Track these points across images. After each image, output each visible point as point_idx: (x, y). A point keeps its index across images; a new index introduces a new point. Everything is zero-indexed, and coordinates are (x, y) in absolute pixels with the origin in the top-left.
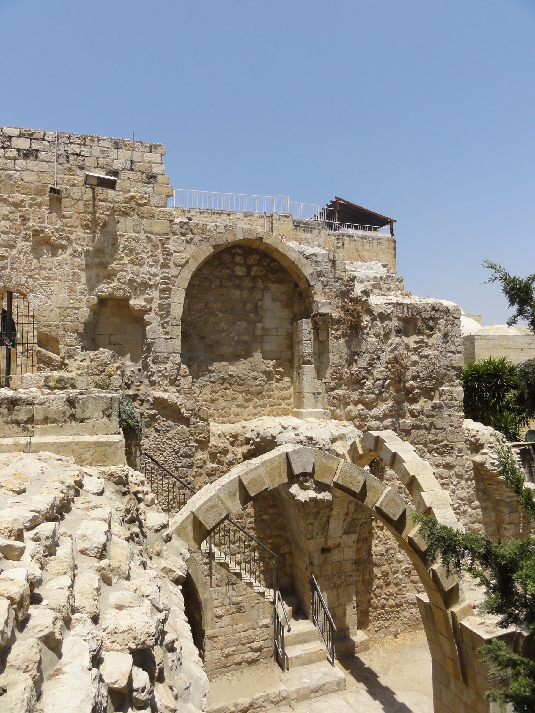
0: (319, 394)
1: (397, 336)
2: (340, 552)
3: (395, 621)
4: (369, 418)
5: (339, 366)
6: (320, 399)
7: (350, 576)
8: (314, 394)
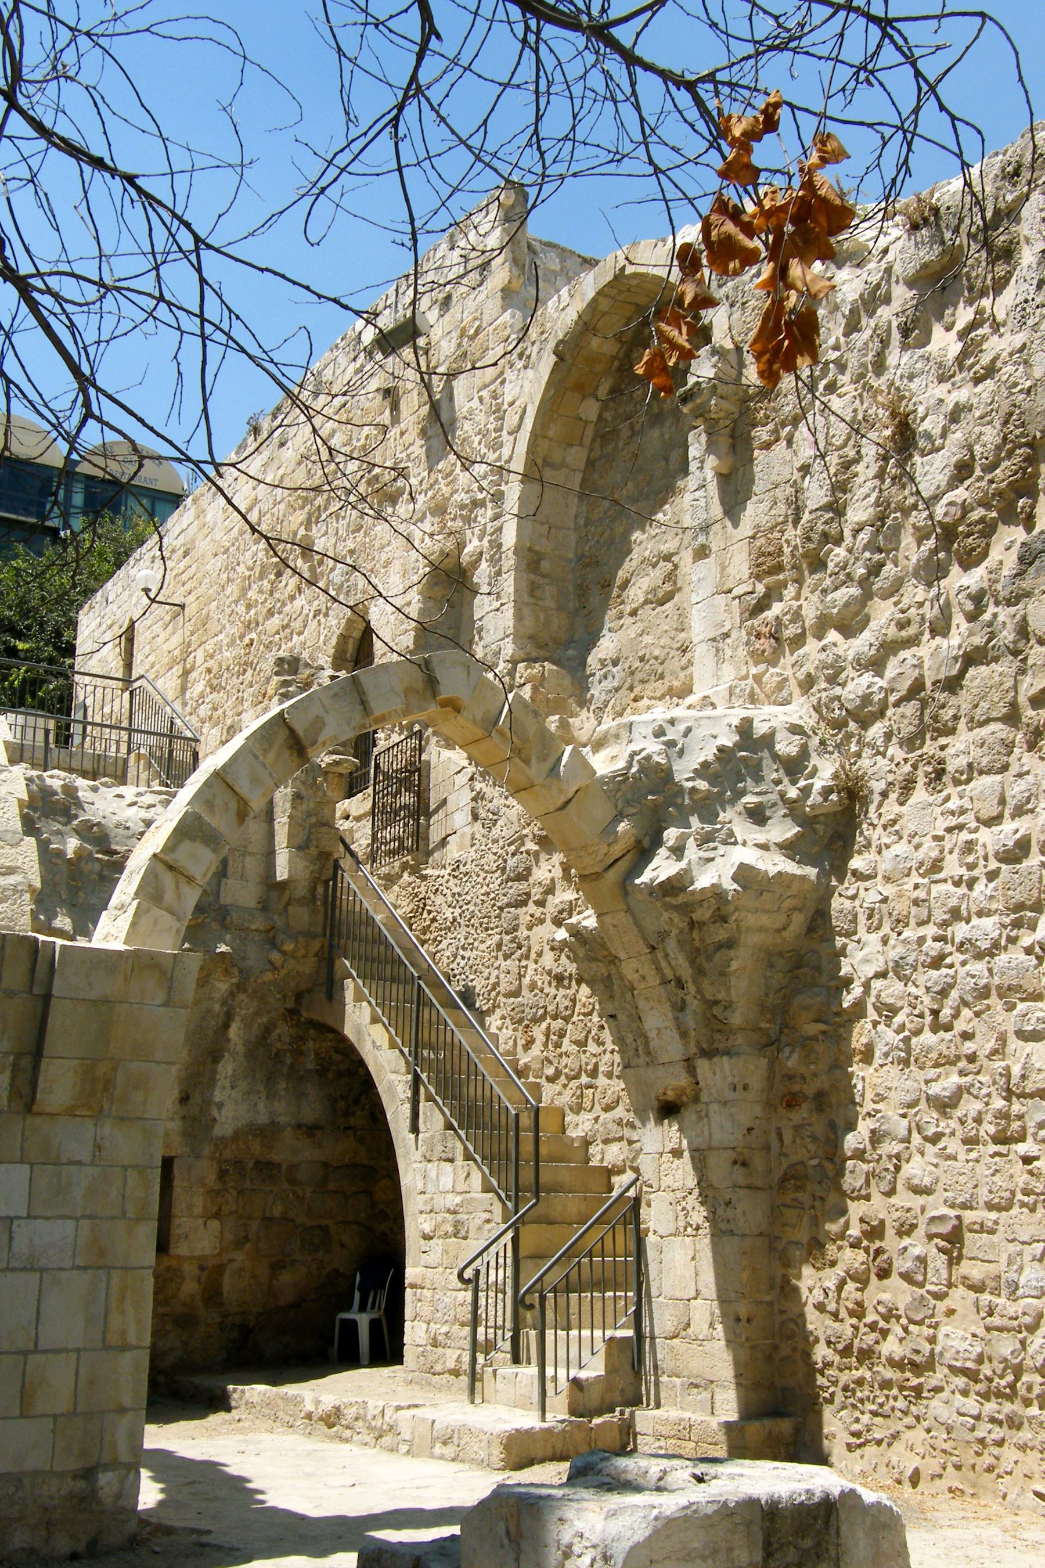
0: (727, 635)
1: (905, 347)
2: (701, 1118)
3: (909, 1427)
4: (850, 672)
5: (772, 529)
6: (728, 652)
7: (728, 1204)
8: (714, 640)
